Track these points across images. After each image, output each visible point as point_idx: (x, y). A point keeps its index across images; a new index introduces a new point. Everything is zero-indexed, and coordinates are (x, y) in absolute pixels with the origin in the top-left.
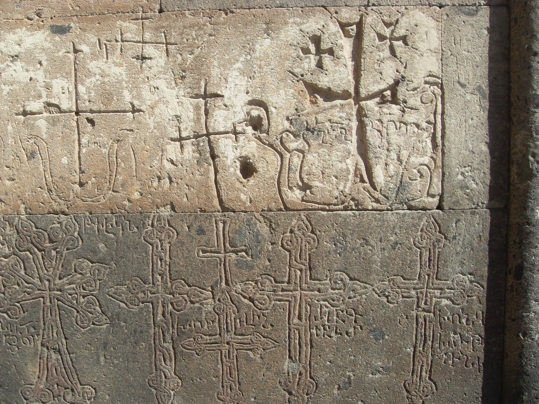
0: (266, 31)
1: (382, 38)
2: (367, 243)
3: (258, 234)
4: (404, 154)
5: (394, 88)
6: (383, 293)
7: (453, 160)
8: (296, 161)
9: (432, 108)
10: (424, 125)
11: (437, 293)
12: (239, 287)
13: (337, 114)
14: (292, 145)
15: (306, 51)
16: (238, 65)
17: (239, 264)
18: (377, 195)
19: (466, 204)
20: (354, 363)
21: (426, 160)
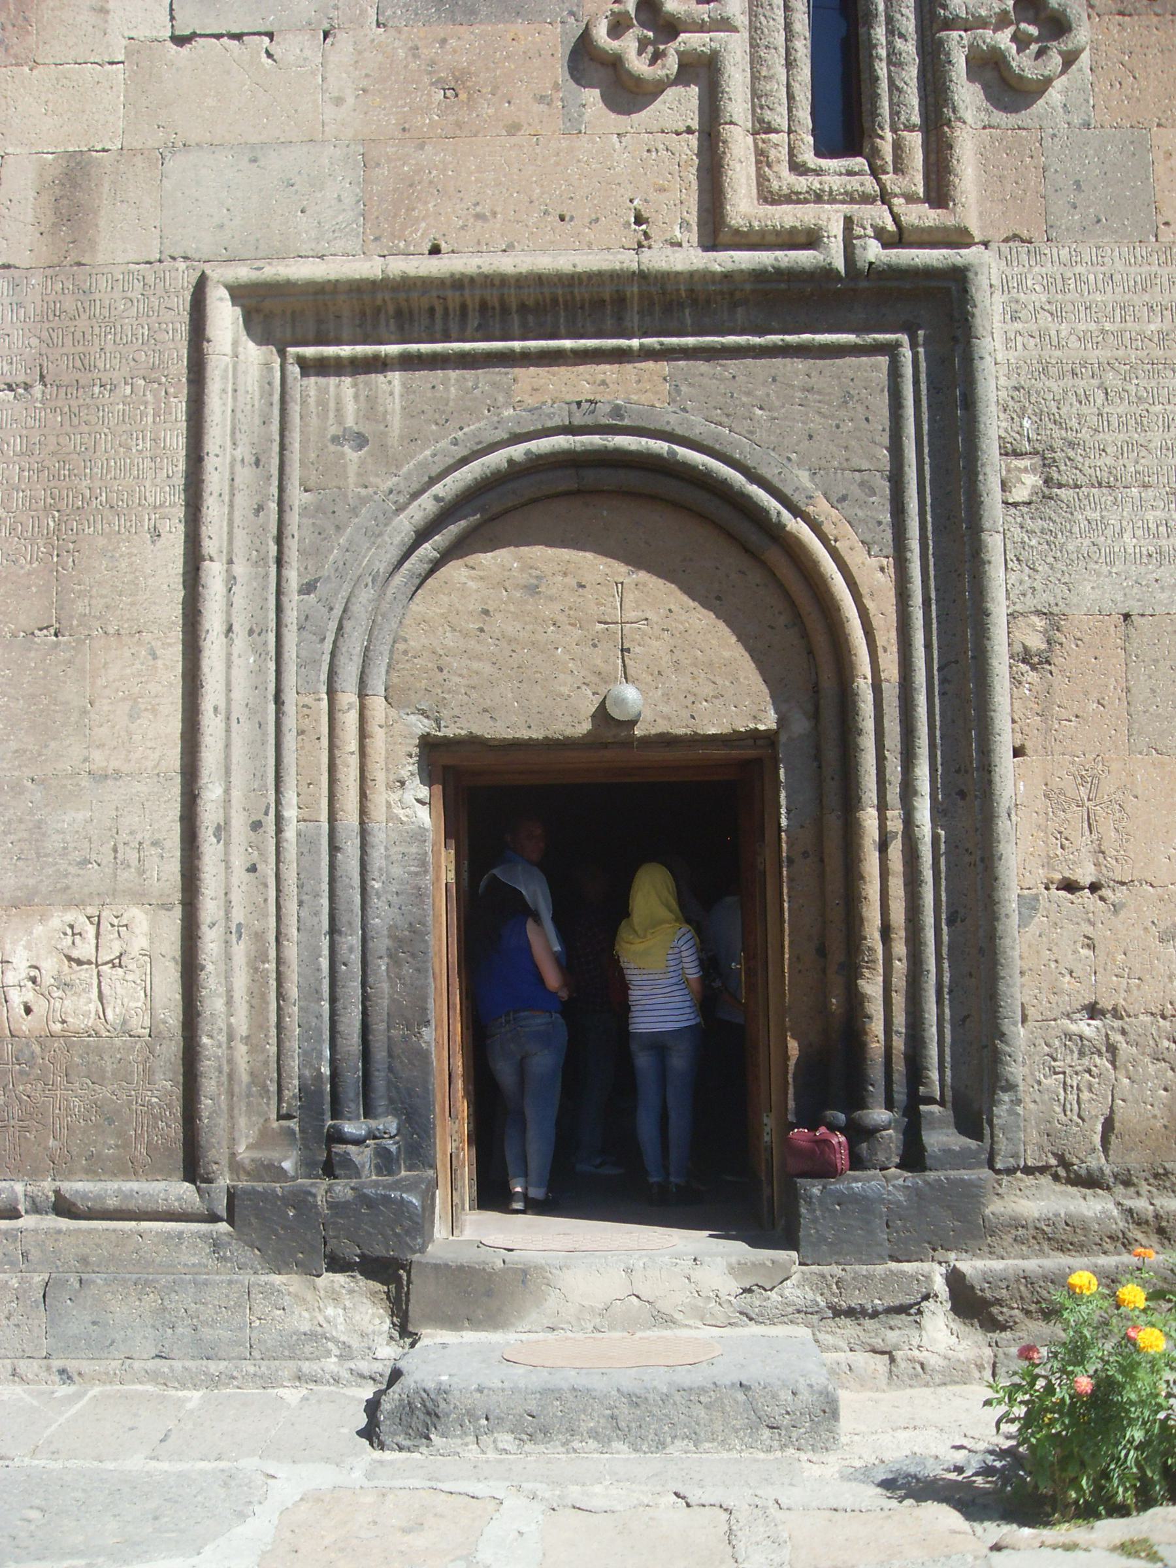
0: (40, 921)
1: (113, 926)
2: (102, 1059)
3: (33, 1053)
4: (126, 1000)
5: (120, 957)
6: (113, 1093)
7: (158, 1005)
8: (58, 1005)
9: (142, 970)
10: (139, 982)
11: (149, 1093)
12: (21, 1088)
13: (83, 975)
14: (55, 995)
15: (65, 934)
16: (22, 943)
17: (21, 1072)
18: (109, 1027)
19: (166, 1034)
20: (95, 1141)
21: (140, 1004)
